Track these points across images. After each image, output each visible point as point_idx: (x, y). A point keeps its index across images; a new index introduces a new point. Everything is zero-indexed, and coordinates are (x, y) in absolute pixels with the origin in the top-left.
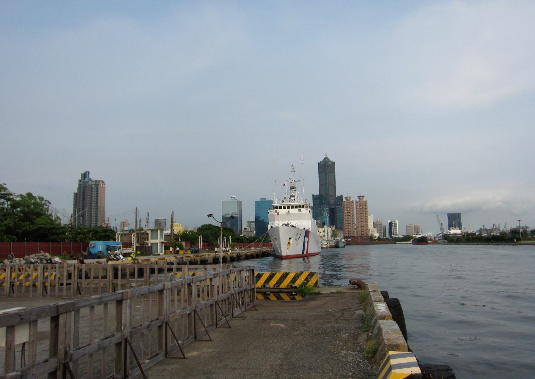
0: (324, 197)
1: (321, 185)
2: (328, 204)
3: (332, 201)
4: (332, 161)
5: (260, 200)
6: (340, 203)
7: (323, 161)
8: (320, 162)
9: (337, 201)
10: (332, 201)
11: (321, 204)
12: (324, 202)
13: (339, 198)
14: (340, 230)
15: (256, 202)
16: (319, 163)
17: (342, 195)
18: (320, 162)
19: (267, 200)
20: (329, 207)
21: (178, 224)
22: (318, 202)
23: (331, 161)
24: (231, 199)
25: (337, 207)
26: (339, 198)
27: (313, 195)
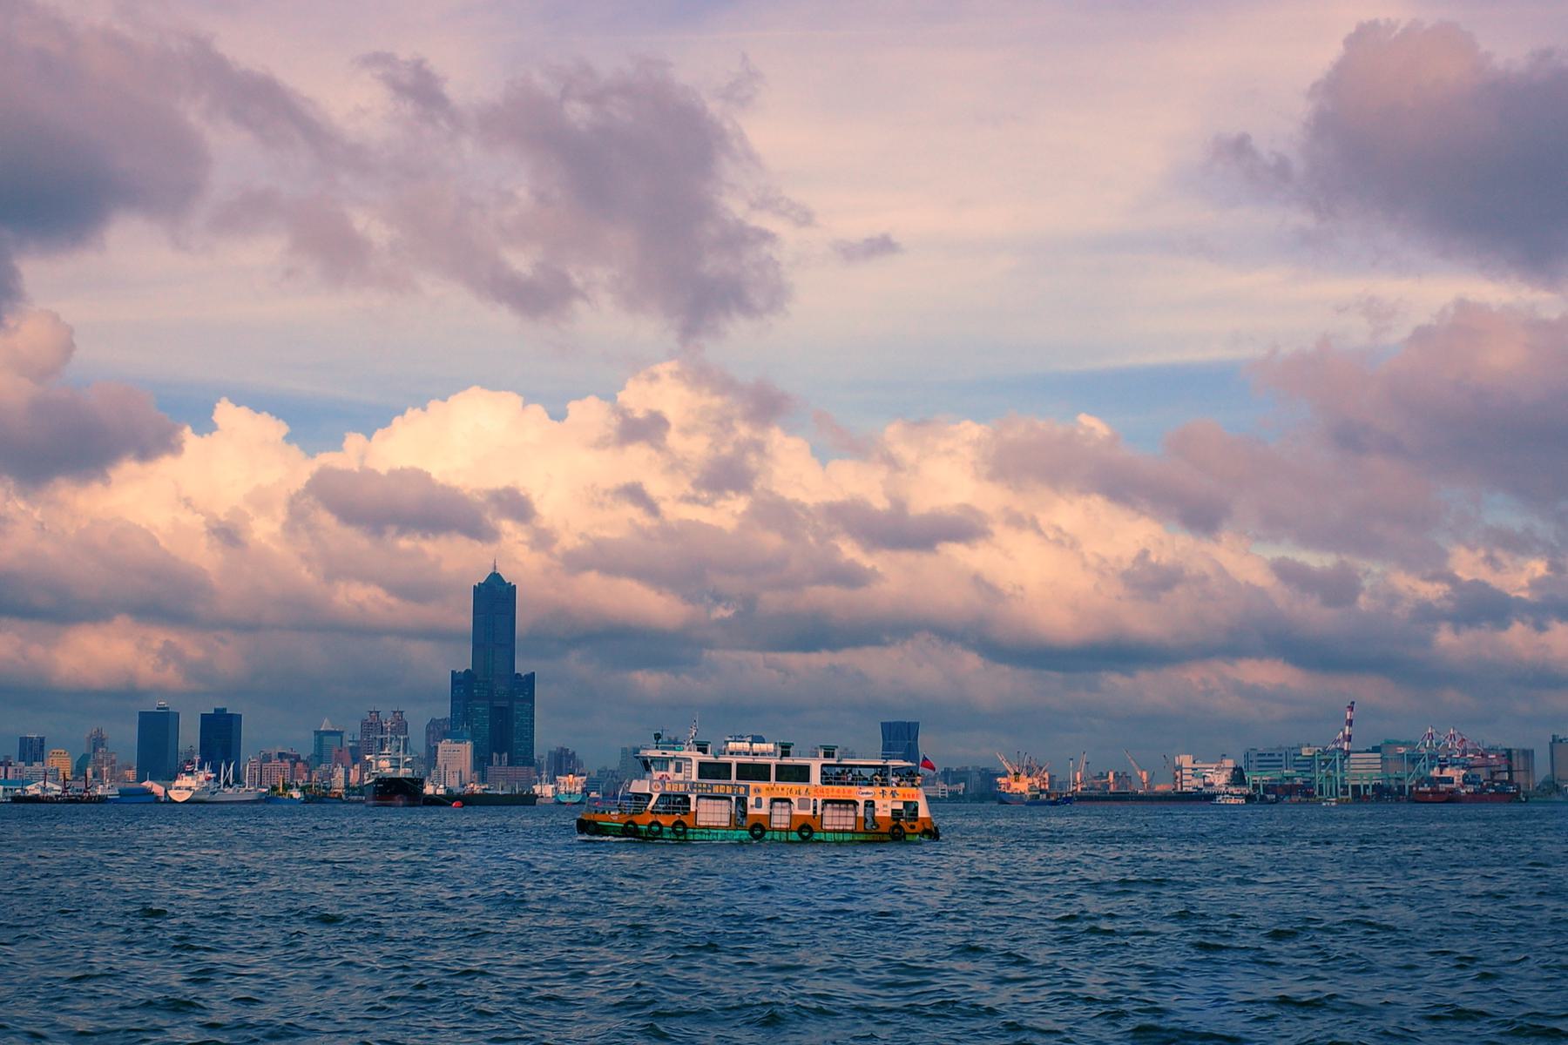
0: (479, 679)
4: (510, 583)
6: (526, 693)
7: (483, 584)
8: (477, 585)
9: (516, 689)
12: (475, 691)
13: (524, 680)
14: (523, 765)
15: (202, 715)
16: (475, 586)
19: (228, 712)
21: (63, 751)
22: (462, 691)
23: (507, 582)
24: (158, 709)
25: (516, 703)
26: (524, 680)
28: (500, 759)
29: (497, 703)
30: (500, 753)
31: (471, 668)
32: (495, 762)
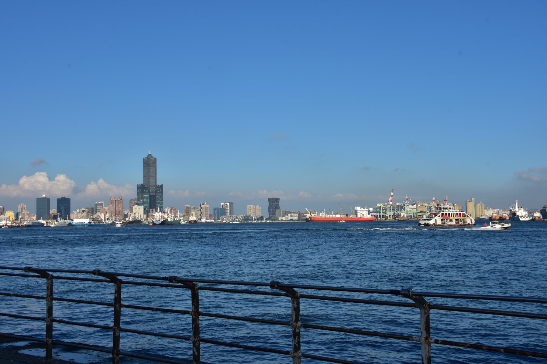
0: (145, 186)
1: (146, 176)
2: (149, 192)
3: (152, 189)
5: (61, 198)
6: (160, 191)
10: (152, 189)
11: (142, 192)
16: (144, 159)
17: (162, 185)
18: (145, 157)
19: (66, 198)
20: (149, 194)
21: (11, 211)
23: (154, 157)
24: (43, 197)
27: (137, 185)
28: (153, 210)
29: (151, 194)
30: (152, 209)
31: (143, 183)
32: (151, 212)
